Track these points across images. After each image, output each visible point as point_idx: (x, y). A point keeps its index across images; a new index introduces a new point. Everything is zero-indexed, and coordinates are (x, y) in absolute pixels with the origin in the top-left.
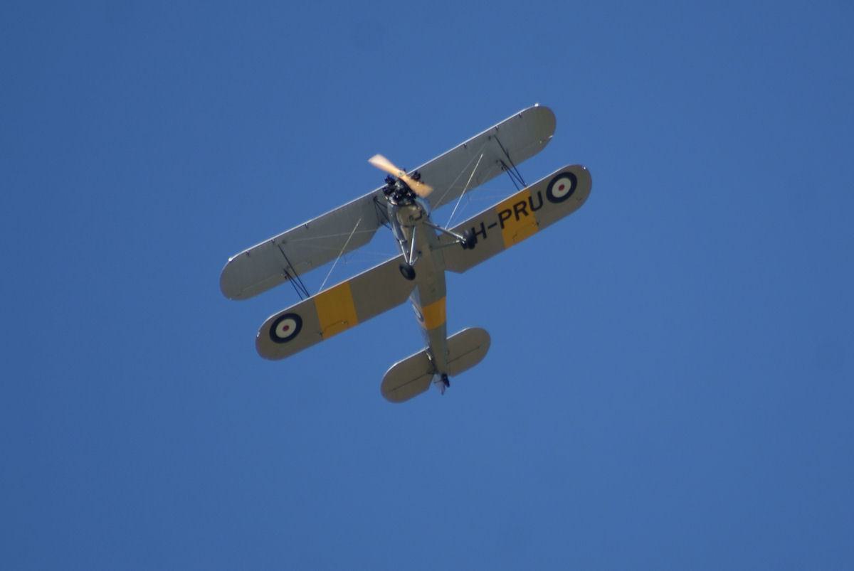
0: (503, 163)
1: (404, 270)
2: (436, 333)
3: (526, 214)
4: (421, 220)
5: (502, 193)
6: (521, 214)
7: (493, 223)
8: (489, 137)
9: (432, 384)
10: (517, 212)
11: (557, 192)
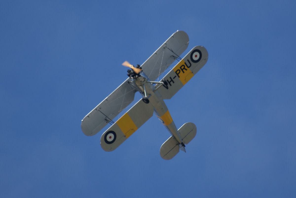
0: (173, 56)
1: (144, 101)
2: (171, 126)
3: (186, 70)
4: (145, 81)
6: (184, 70)
7: (175, 76)
8: (164, 48)
9: (180, 150)
10: (182, 70)
11: (195, 59)
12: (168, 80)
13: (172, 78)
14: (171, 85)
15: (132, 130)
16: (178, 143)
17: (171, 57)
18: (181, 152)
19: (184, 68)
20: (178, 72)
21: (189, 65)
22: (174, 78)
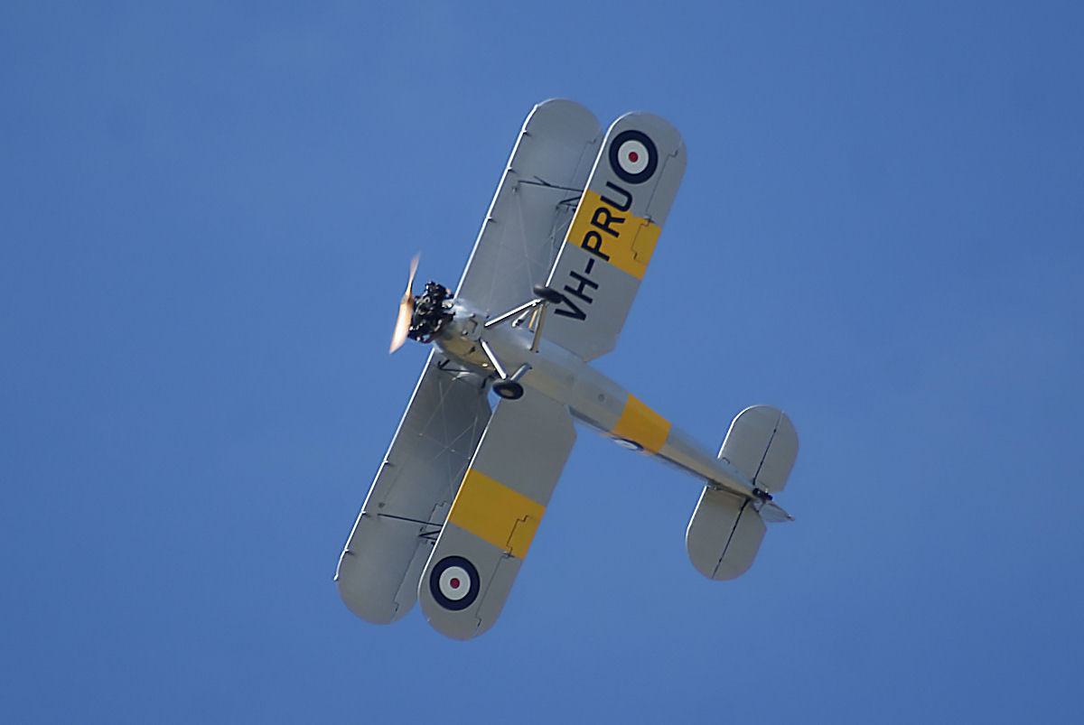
3: (622, 220)
5: (578, 224)
6: (612, 225)
9: (767, 524)
10: (605, 227)
12: (567, 288)
14: (590, 301)
16: (744, 500)
17: (557, 208)
18: (774, 530)
19: (610, 219)
20: (592, 242)
21: (623, 200)
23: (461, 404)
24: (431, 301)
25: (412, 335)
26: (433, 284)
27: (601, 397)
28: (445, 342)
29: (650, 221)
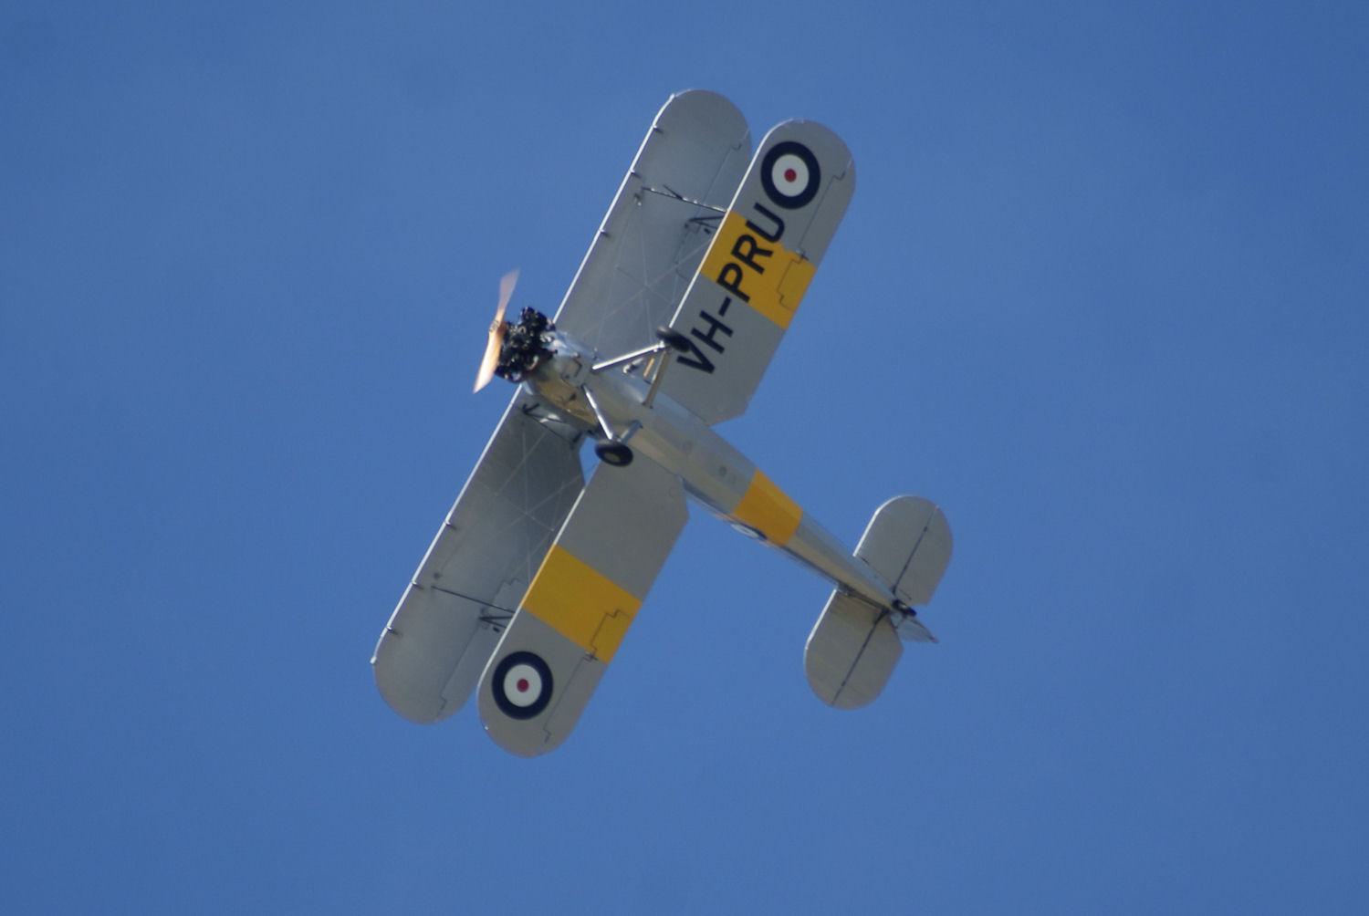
2: (804, 545)
3: (768, 253)
6: (757, 259)
10: (748, 260)
12: (695, 332)
13: (715, 315)
14: (720, 349)
15: (615, 615)
16: (880, 611)
20: (731, 277)
21: (772, 228)
22: (722, 311)
23: (545, 460)
24: (528, 332)
25: (500, 371)
26: (531, 310)
27: (723, 470)
28: (540, 384)
29: (803, 256)
